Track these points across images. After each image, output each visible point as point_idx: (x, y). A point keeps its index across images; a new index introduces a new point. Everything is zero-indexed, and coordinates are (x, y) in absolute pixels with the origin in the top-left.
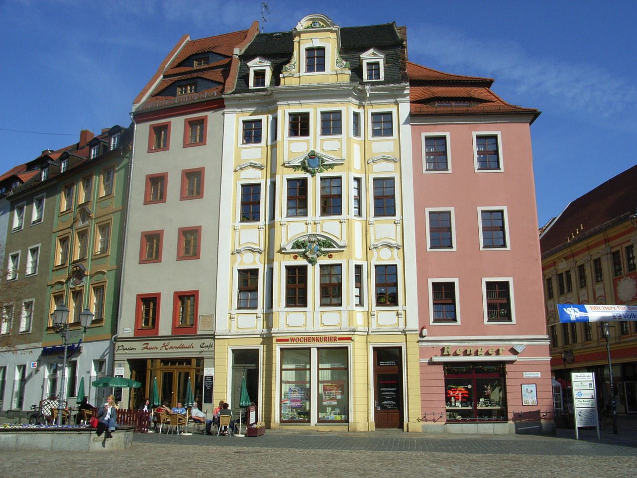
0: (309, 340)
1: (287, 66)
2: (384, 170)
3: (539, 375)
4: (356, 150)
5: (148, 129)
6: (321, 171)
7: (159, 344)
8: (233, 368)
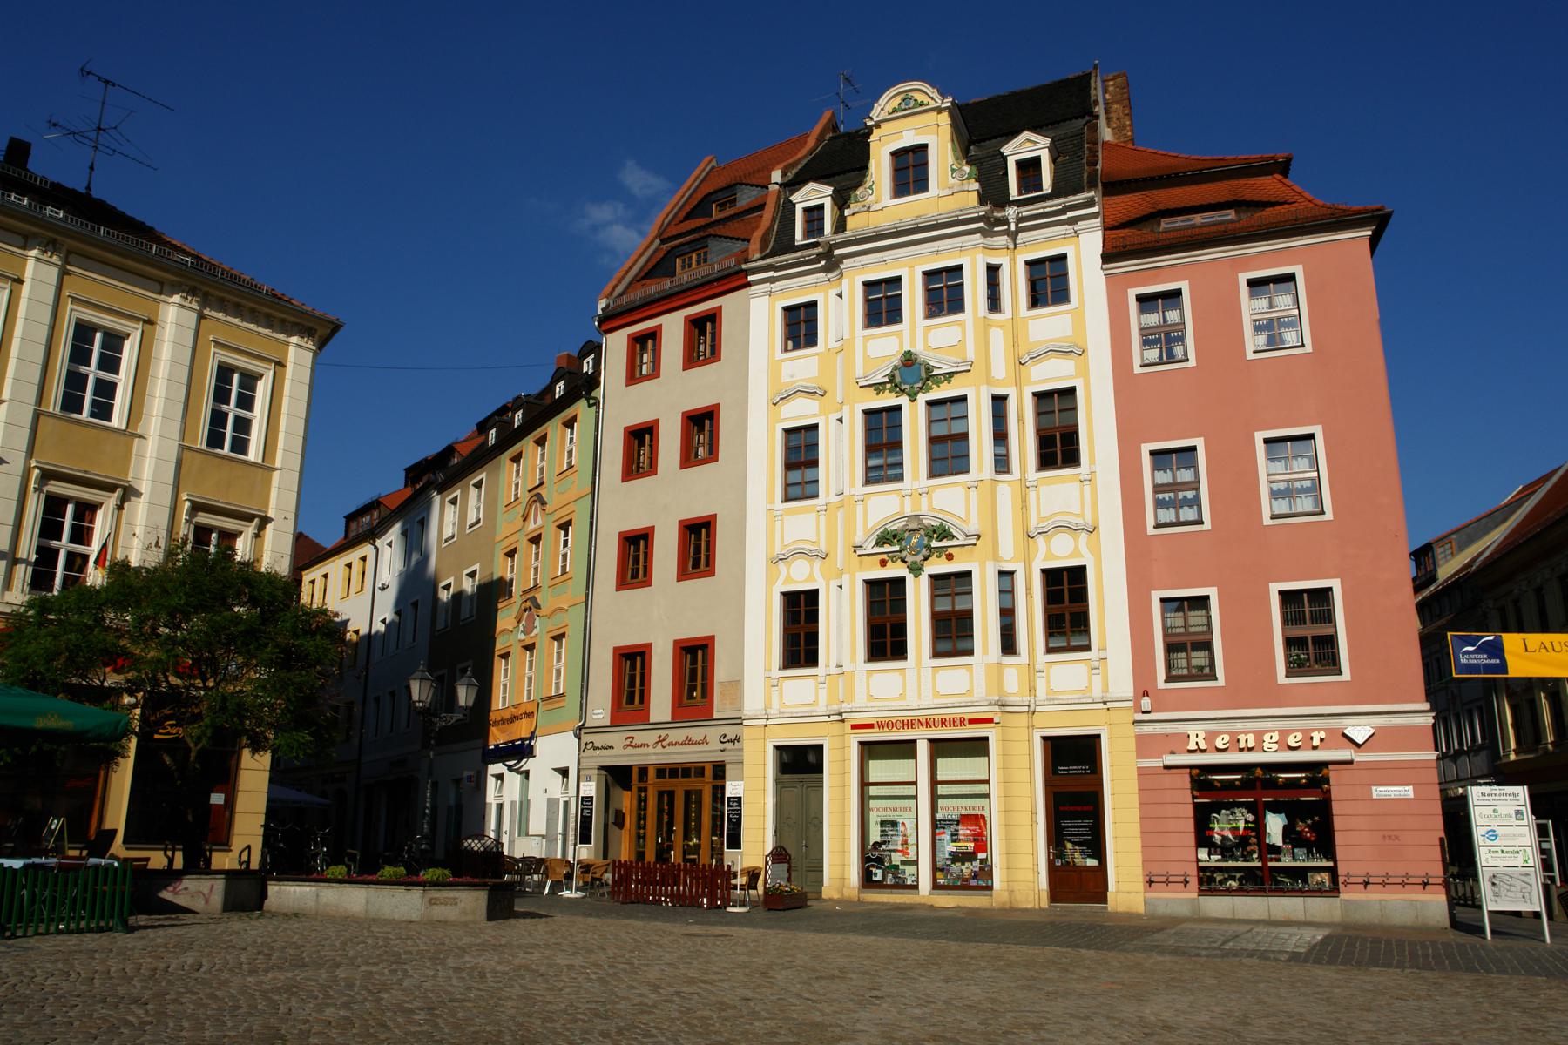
0: (912, 724)
1: (858, 192)
2: (1052, 374)
3: (1408, 791)
4: (998, 337)
7: (650, 737)
8: (777, 781)
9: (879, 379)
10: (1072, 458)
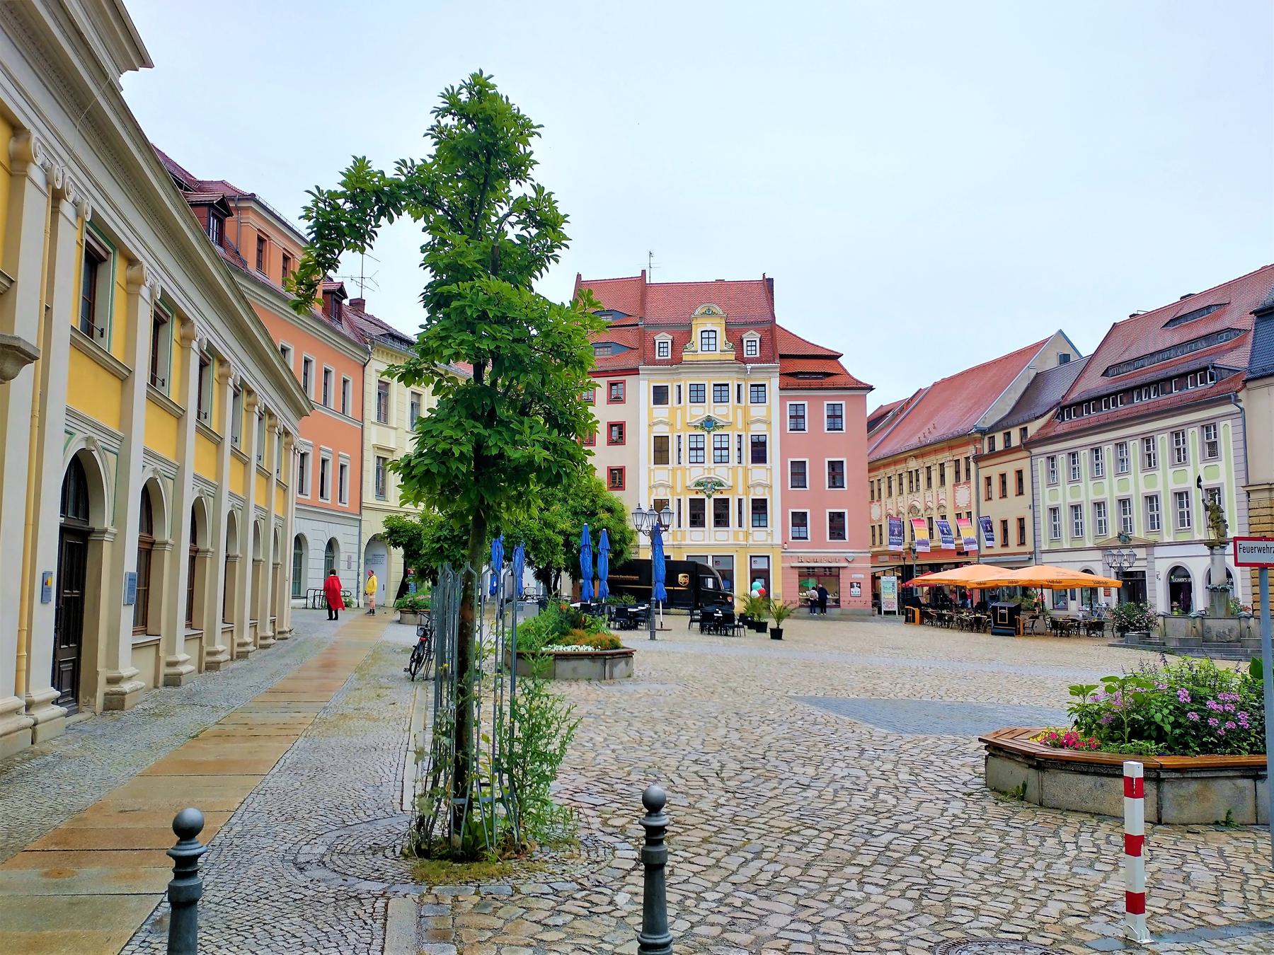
2: (758, 429)
6: (714, 430)
10: (763, 460)
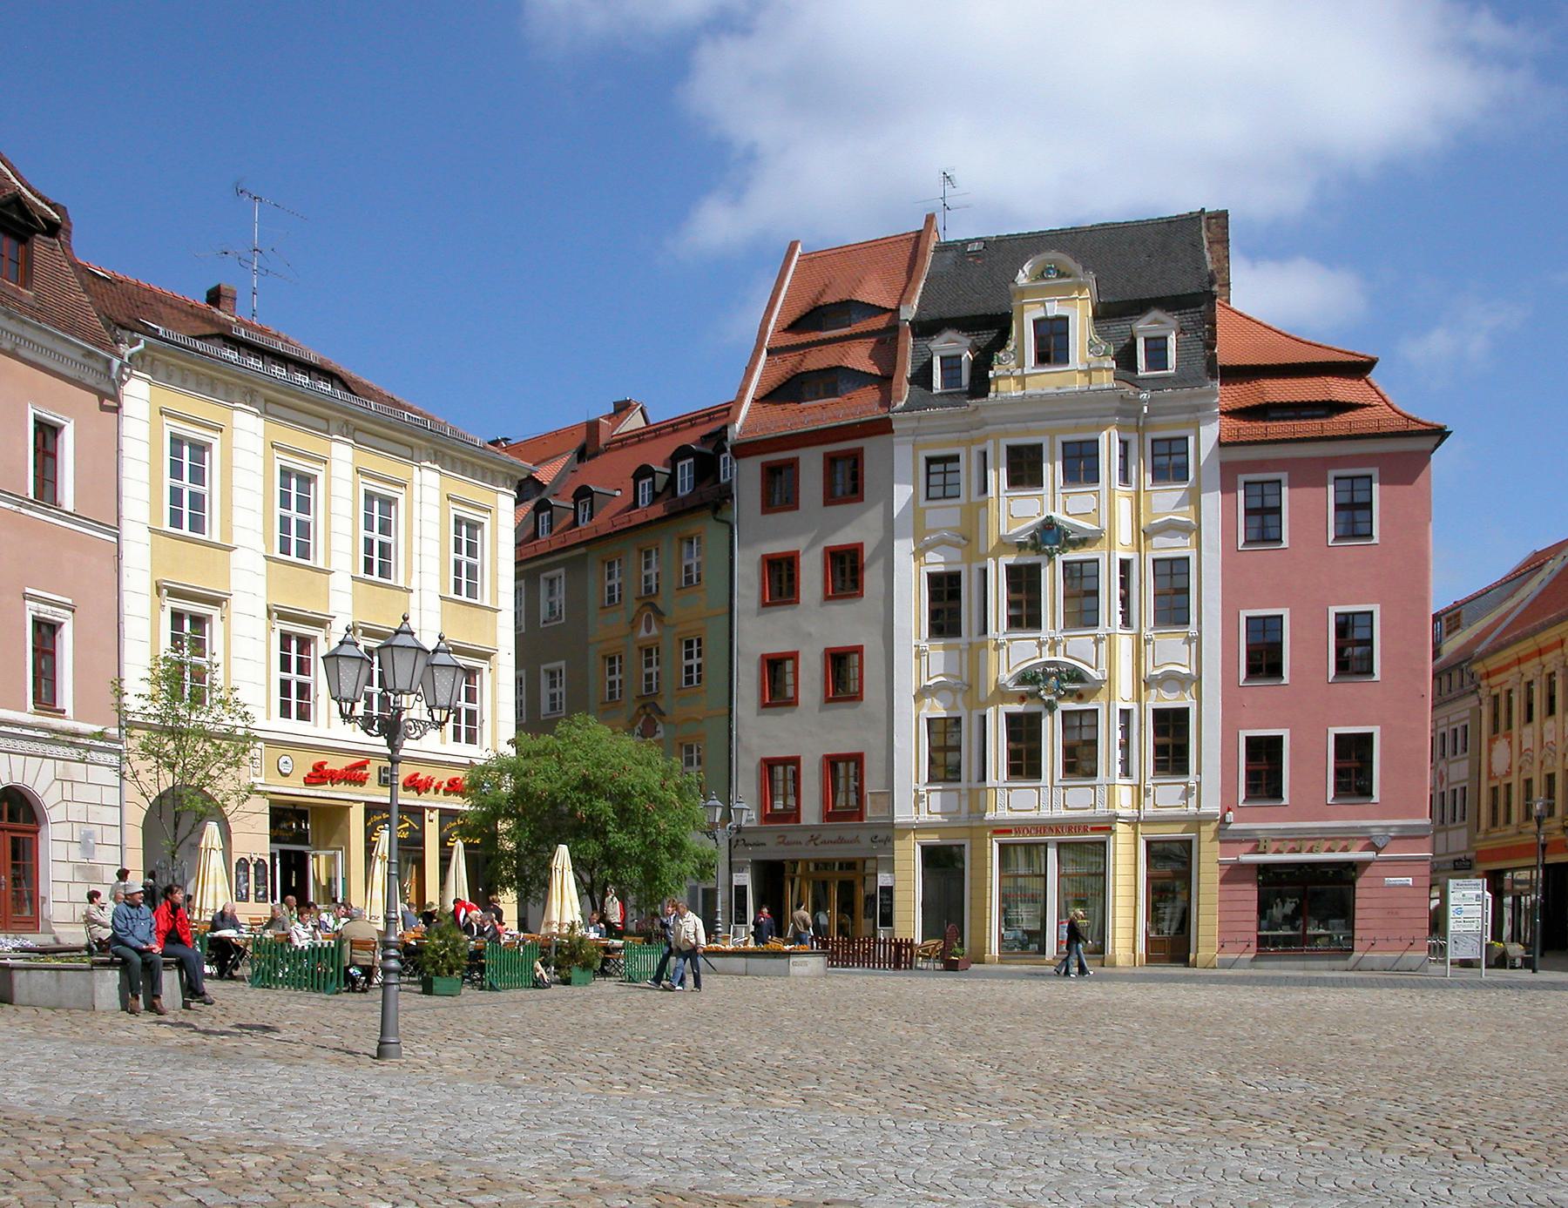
1: (1001, 355)
4: (1124, 507)
5: (758, 470)
6: (1062, 550)
9: (1024, 538)
